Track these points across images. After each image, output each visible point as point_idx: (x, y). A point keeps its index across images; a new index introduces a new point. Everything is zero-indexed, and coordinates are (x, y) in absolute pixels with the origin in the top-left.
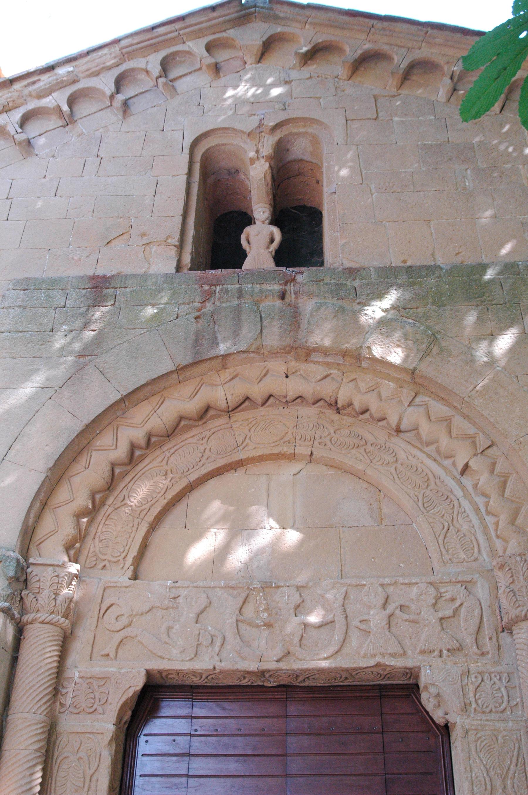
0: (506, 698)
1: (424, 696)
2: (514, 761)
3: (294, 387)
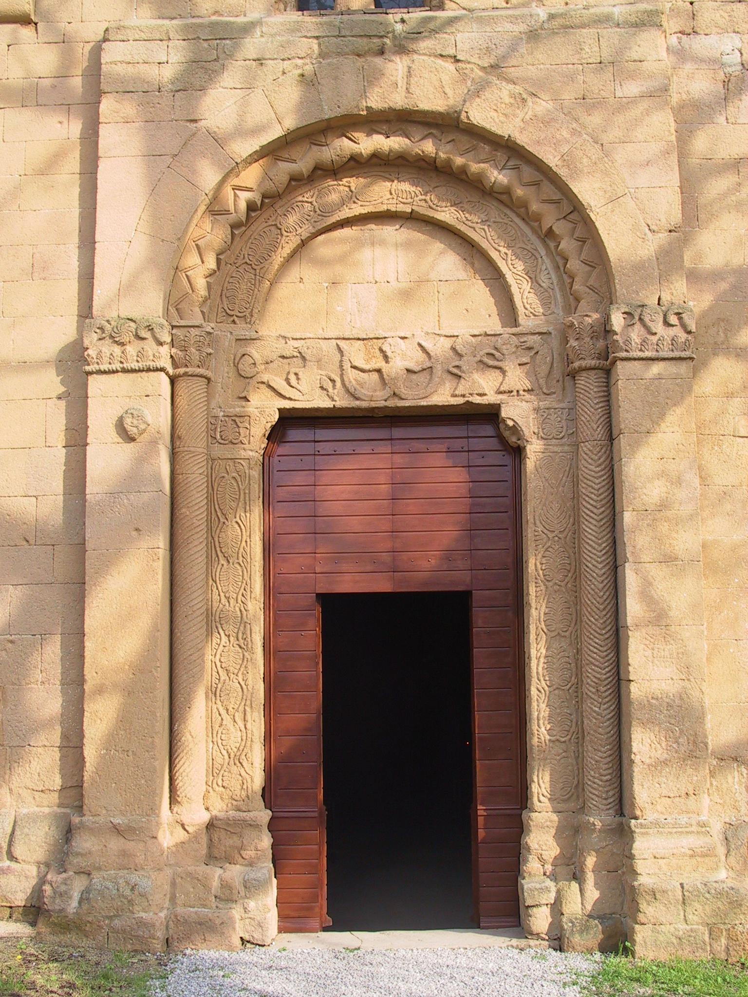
0: (565, 428)
1: (501, 426)
2: (566, 474)
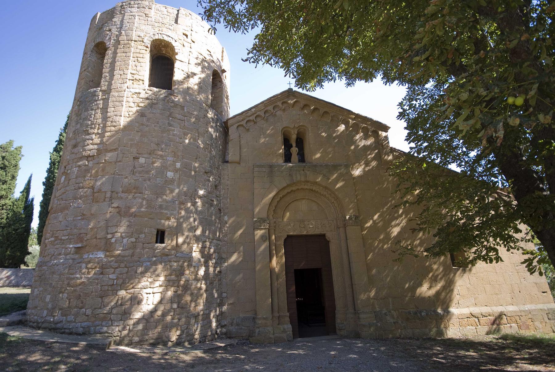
3: (306, 187)
